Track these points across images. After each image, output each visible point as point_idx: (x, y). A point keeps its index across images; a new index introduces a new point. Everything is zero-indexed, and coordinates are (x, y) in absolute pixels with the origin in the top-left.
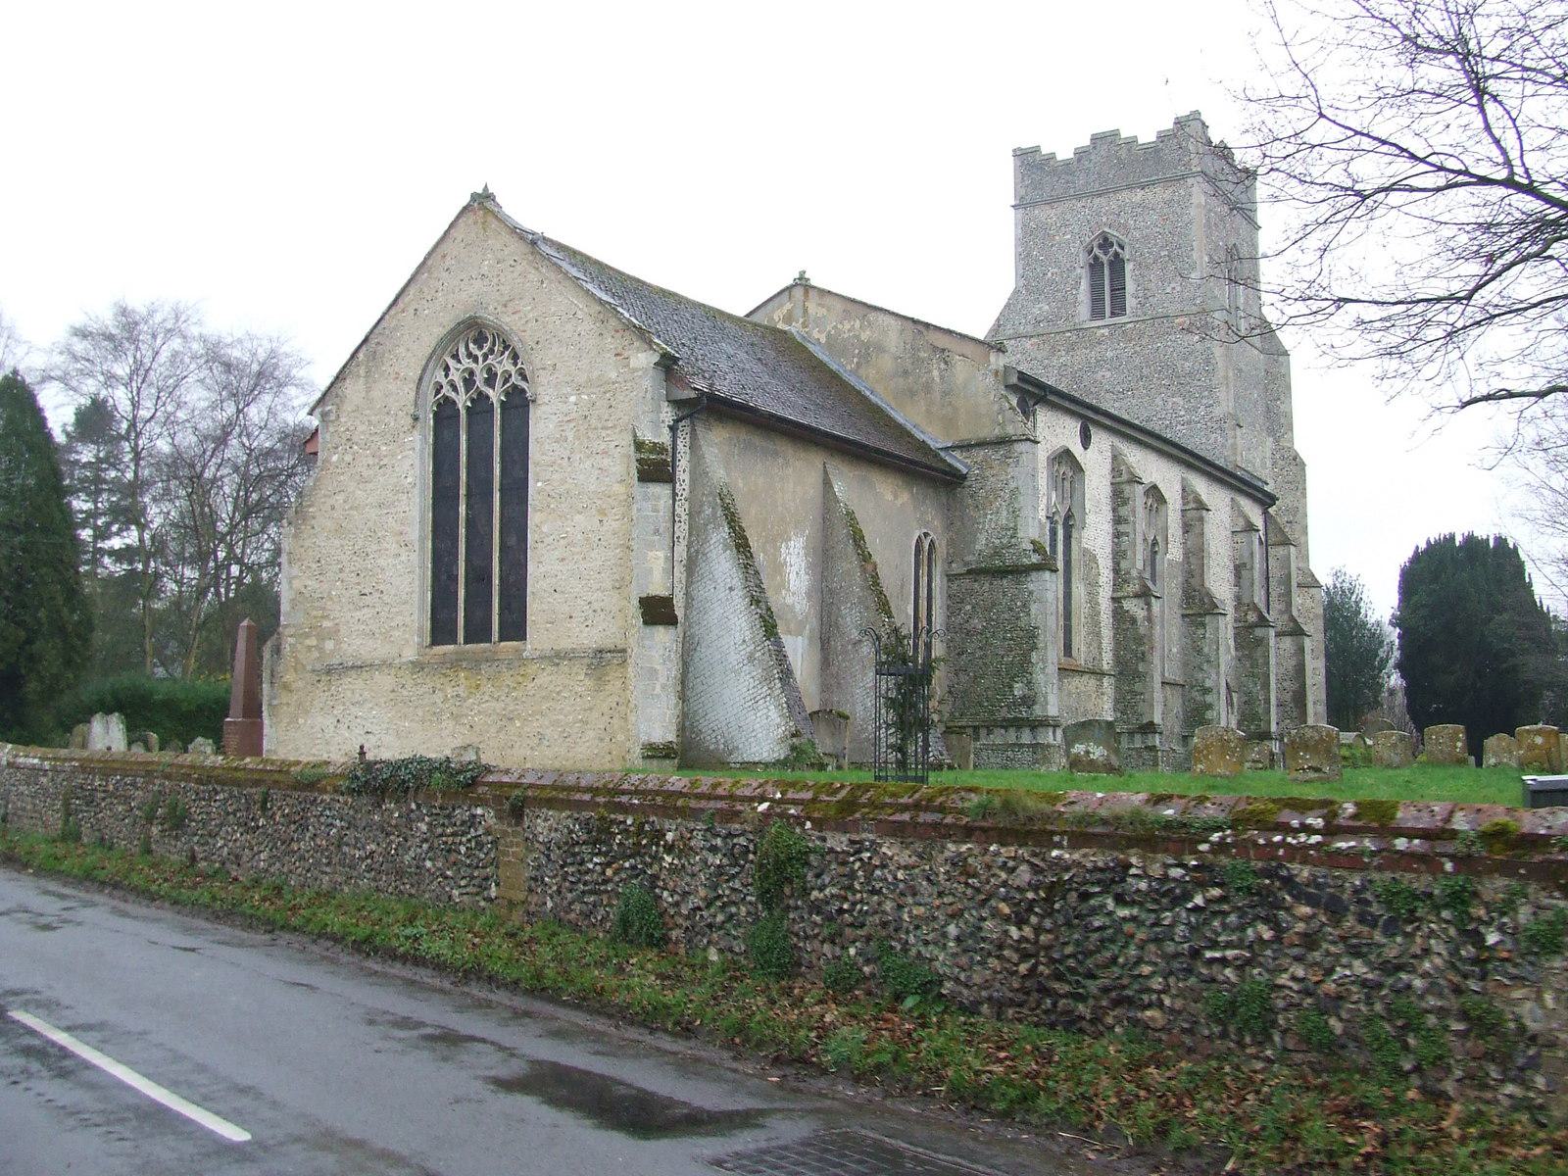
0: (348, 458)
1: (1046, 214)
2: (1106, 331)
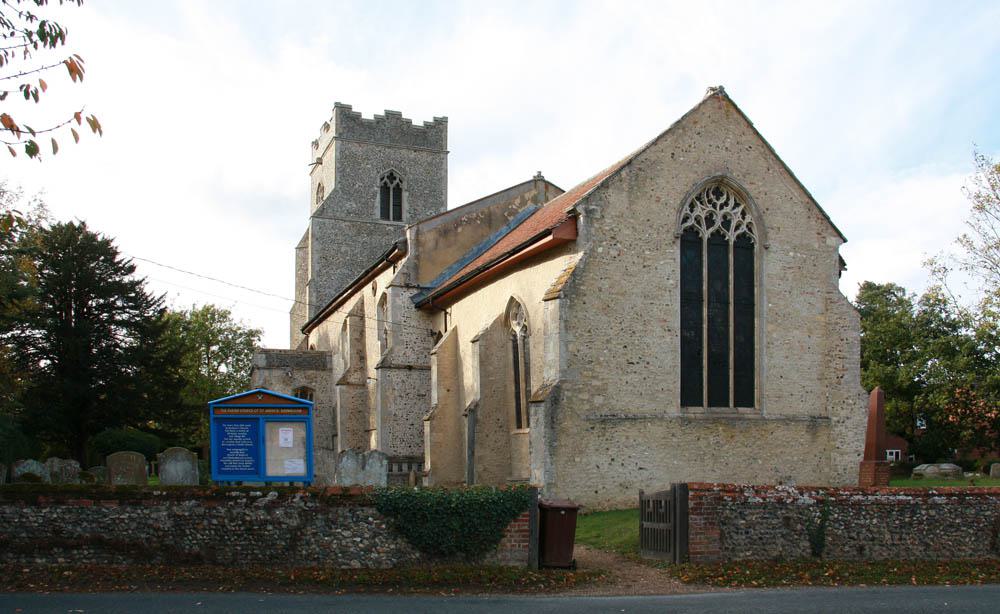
0: (614, 253)
1: (355, 148)
2: (392, 228)
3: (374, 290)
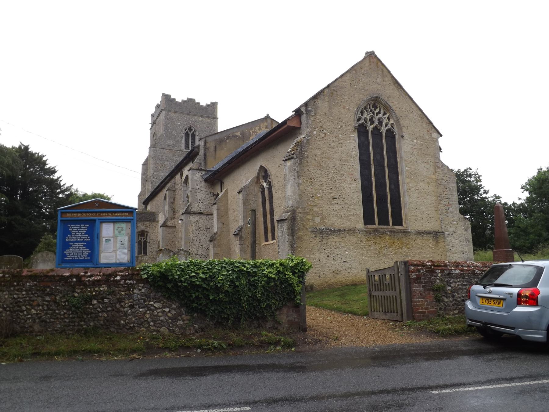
0: (322, 135)
3: (182, 176)
